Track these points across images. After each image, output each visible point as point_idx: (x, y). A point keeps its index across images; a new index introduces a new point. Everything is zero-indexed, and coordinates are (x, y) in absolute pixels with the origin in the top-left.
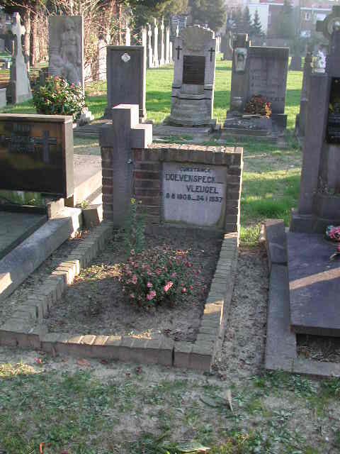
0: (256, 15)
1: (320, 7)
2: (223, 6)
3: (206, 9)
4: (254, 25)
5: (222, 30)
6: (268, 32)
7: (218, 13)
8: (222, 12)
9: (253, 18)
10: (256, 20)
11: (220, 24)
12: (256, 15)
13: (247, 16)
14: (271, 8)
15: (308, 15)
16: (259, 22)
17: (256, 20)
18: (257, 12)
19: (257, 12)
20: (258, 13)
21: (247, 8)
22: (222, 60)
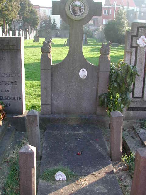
0: (54, 20)
3: (29, 17)
5: (38, 27)
6: (60, 27)
8: (37, 18)
9: (52, 21)
10: (54, 22)
11: (37, 24)
12: (54, 20)
13: (50, 20)
16: (55, 23)
17: (54, 22)
18: (54, 18)
19: (54, 18)
20: (55, 19)
21: (50, 16)
22: (34, 41)
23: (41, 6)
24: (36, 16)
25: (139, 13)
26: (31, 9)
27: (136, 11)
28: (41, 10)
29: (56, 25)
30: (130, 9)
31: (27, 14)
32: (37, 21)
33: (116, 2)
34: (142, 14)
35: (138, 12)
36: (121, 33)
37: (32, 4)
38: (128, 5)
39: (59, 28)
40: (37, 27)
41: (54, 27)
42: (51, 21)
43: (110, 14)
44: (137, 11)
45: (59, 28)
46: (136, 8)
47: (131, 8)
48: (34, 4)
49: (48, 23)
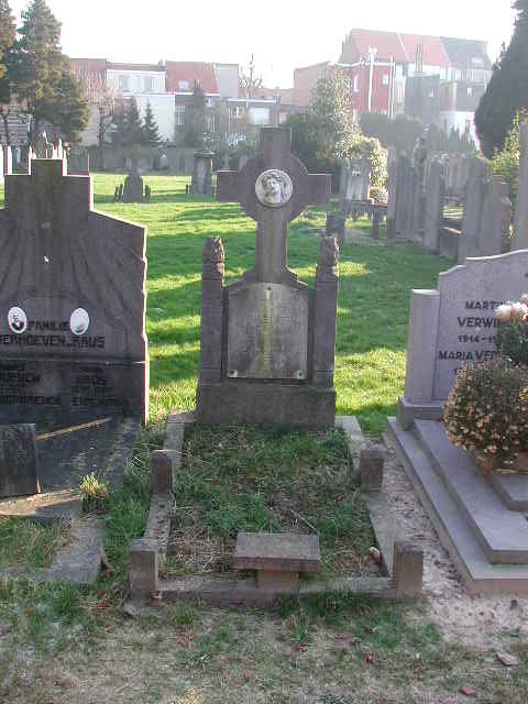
0: (149, 111)
1: (263, 98)
2: (83, 97)
3: (55, 100)
4: (146, 126)
6: (176, 138)
7: (73, 107)
9: (142, 115)
10: (149, 117)
11: (81, 126)
12: (149, 111)
13: (134, 113)
14: (179, 100)
15: (240, 110)
16: (153, 121)
17: (149, 117)
18: (148, 105)
19: (148, 105)
23: (114, 60)
24: (76, 95)
25: (458, 90)
26: (60, 73)
27: (449, 79)
28: (111, 75)
29: (156, 130)
30: (428, 75)
31: (44, 90)
32: (81, 114)
33: (375, 50)
34: (469, 90)
35: (455, 84)
36: (326, 156)
37: (62, 58)
38: (420, 60)
39: (171, 140)
40: (81, 134)
41: (147, 136)
42: (137, 114)
43: (356, 90)
44: (450, 83)
45: (171, 140)
46: (450, 69)
47: (429, 70)
48: (72, 56)
49: (126, 120)
